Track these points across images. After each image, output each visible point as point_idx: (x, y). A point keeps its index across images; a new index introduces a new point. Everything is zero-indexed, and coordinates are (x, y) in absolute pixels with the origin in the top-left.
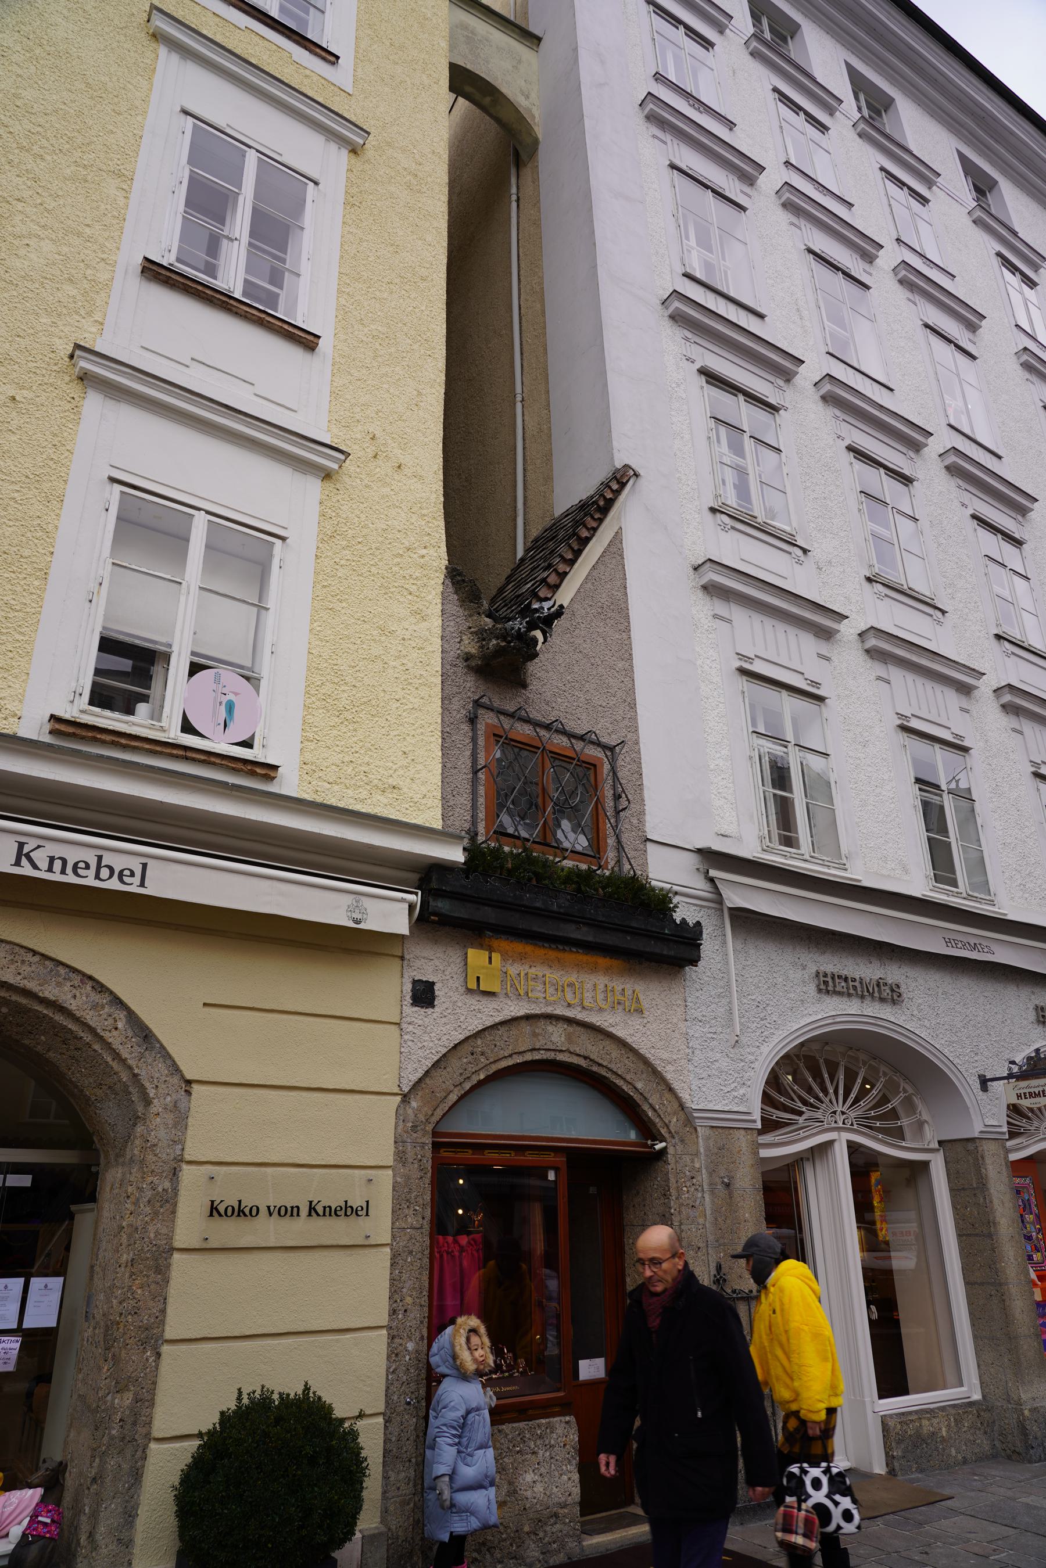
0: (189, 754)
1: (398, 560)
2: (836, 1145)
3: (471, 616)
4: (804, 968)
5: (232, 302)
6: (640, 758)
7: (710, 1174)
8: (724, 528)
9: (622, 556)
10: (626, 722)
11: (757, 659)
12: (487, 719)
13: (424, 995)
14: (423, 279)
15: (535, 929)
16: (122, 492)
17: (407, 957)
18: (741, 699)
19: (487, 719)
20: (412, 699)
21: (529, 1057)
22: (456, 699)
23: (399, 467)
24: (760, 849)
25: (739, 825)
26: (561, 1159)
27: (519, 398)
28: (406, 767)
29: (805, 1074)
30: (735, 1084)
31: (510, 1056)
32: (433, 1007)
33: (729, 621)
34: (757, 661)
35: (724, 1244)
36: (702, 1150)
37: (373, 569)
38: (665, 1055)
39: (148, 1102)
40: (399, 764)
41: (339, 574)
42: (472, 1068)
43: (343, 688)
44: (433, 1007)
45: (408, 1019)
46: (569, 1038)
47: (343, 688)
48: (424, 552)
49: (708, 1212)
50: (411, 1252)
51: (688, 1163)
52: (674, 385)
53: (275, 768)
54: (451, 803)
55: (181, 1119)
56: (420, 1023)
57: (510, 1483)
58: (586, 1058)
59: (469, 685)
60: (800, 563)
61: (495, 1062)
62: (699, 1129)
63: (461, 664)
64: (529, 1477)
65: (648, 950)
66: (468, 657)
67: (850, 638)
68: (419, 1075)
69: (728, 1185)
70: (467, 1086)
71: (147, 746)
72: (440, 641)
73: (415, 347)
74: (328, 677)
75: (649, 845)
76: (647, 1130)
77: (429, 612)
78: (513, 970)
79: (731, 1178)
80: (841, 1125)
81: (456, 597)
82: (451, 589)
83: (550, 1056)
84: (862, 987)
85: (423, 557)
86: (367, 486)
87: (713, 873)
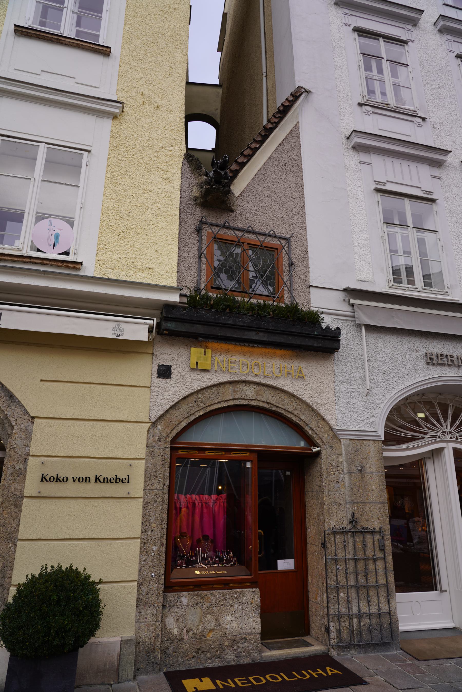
0: (32, 260)
1: (156, 154)
2: (446, 450)
3: (197, 177)
4: (417, 351)
5: (61, 38)
6: (307, 243)
7: (349, 465)
8: (368, 113)
9: (299, 137)
10: (299, 225)
11: (388, 183)
13: (165, 372)
14: (175, 9)
15: (229, 335)
16: (2, 140)
17: (155, 353)
18: (377, 206)
19: (206, 230)
20: (162, 223)
21: (231, 403)
22: (189, 221)
23: (158, 107)
24: (387, 287)
25: (373, 275)
26: (254, 456)
27: (264, 75)
28: (157, 258)
30: (367, 416)
31: (220, 402)
32: (170, 378)
33: (370, 164)
34: (388, 184)
35: (358, 503)
36: (343, 452)
37: (141, 161)
38: (320, 401)
39: (12, 427)
40: (153, 257)
41: (121, 165)
42: (194, 409)
43: (122, 221)
44: (170, 378)
45: (155, 385)
46: (257, 393)
47: (122, 221)
48: (172, 148)
49: (347, 485)
50: (156, 502)
52: (336, 41)
53: (81, 263)
54: (185, 274)
55: (28, 435)
56: (162, 386)
57: (216, 620)
58: (268, 403)
59: (197, 213)
60: (419, 126)
61: (209, 406)
62: (342, 440)
63: (192, 203)
64: (229, 618)
65: (304, 344)
66: (196, 199)
67: (456, 165)
68: (162, 412)
69: (361, 471)
70: (192, 418)
71: (10, 258)
72: (179, 192)
73: (169, 45)
74: (113, 217)
75: (311, 288)
76: (311, 442)
77: (173, 178)
78: (219, 358)
79: (362, 467)
80: (449, 439)
81: (190, 169)
82: (187, 165)
83: (245, 402)
84: (458, 361)
85: (171, 151)
86: (138, 119)
87: (353, 301)
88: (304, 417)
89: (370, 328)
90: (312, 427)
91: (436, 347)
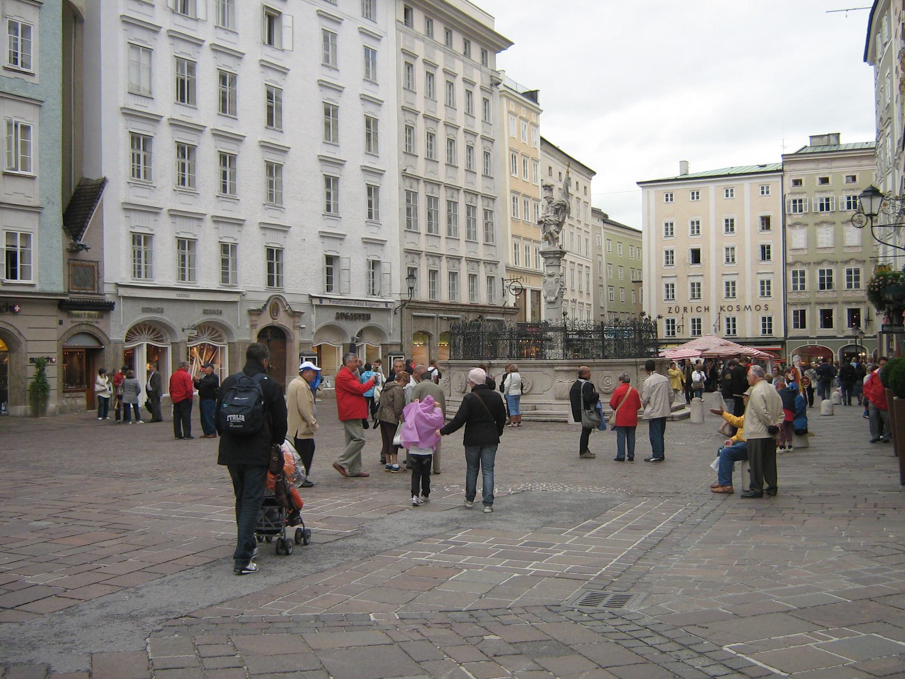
8: (131, 187)
12: (72, 262)
13: (61, 323)
29: (135, 331)
51: (109, 351)
55: (26, 346)
76: (101, 344)
88: (100, 335)
89: (124, 298)
90: (103, 339)
91: (146, 305)
